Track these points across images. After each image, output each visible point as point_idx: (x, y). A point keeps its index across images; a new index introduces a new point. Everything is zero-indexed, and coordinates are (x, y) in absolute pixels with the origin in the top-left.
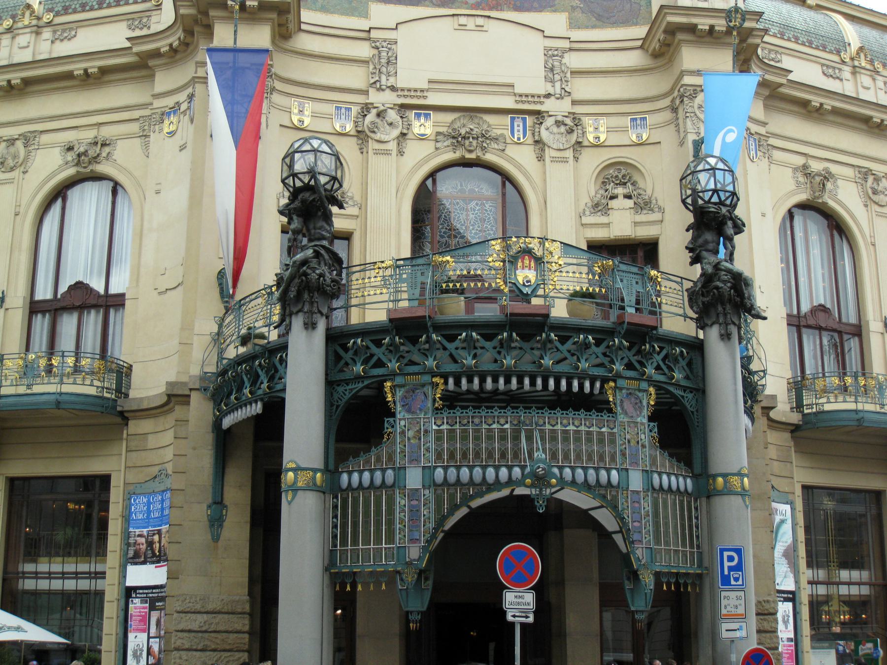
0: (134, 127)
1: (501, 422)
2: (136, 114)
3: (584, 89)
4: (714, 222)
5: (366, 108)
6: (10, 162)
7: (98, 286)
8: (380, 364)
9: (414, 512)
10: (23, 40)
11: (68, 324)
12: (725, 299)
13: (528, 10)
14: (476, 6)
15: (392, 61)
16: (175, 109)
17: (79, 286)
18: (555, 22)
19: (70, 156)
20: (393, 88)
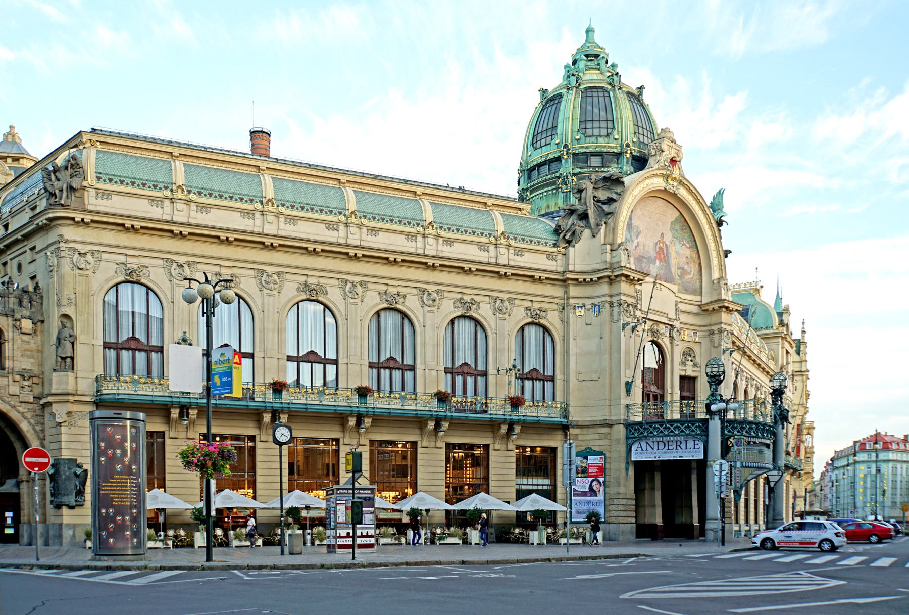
0: (555, 306)
2: (557, 301)
13: (670, 283)
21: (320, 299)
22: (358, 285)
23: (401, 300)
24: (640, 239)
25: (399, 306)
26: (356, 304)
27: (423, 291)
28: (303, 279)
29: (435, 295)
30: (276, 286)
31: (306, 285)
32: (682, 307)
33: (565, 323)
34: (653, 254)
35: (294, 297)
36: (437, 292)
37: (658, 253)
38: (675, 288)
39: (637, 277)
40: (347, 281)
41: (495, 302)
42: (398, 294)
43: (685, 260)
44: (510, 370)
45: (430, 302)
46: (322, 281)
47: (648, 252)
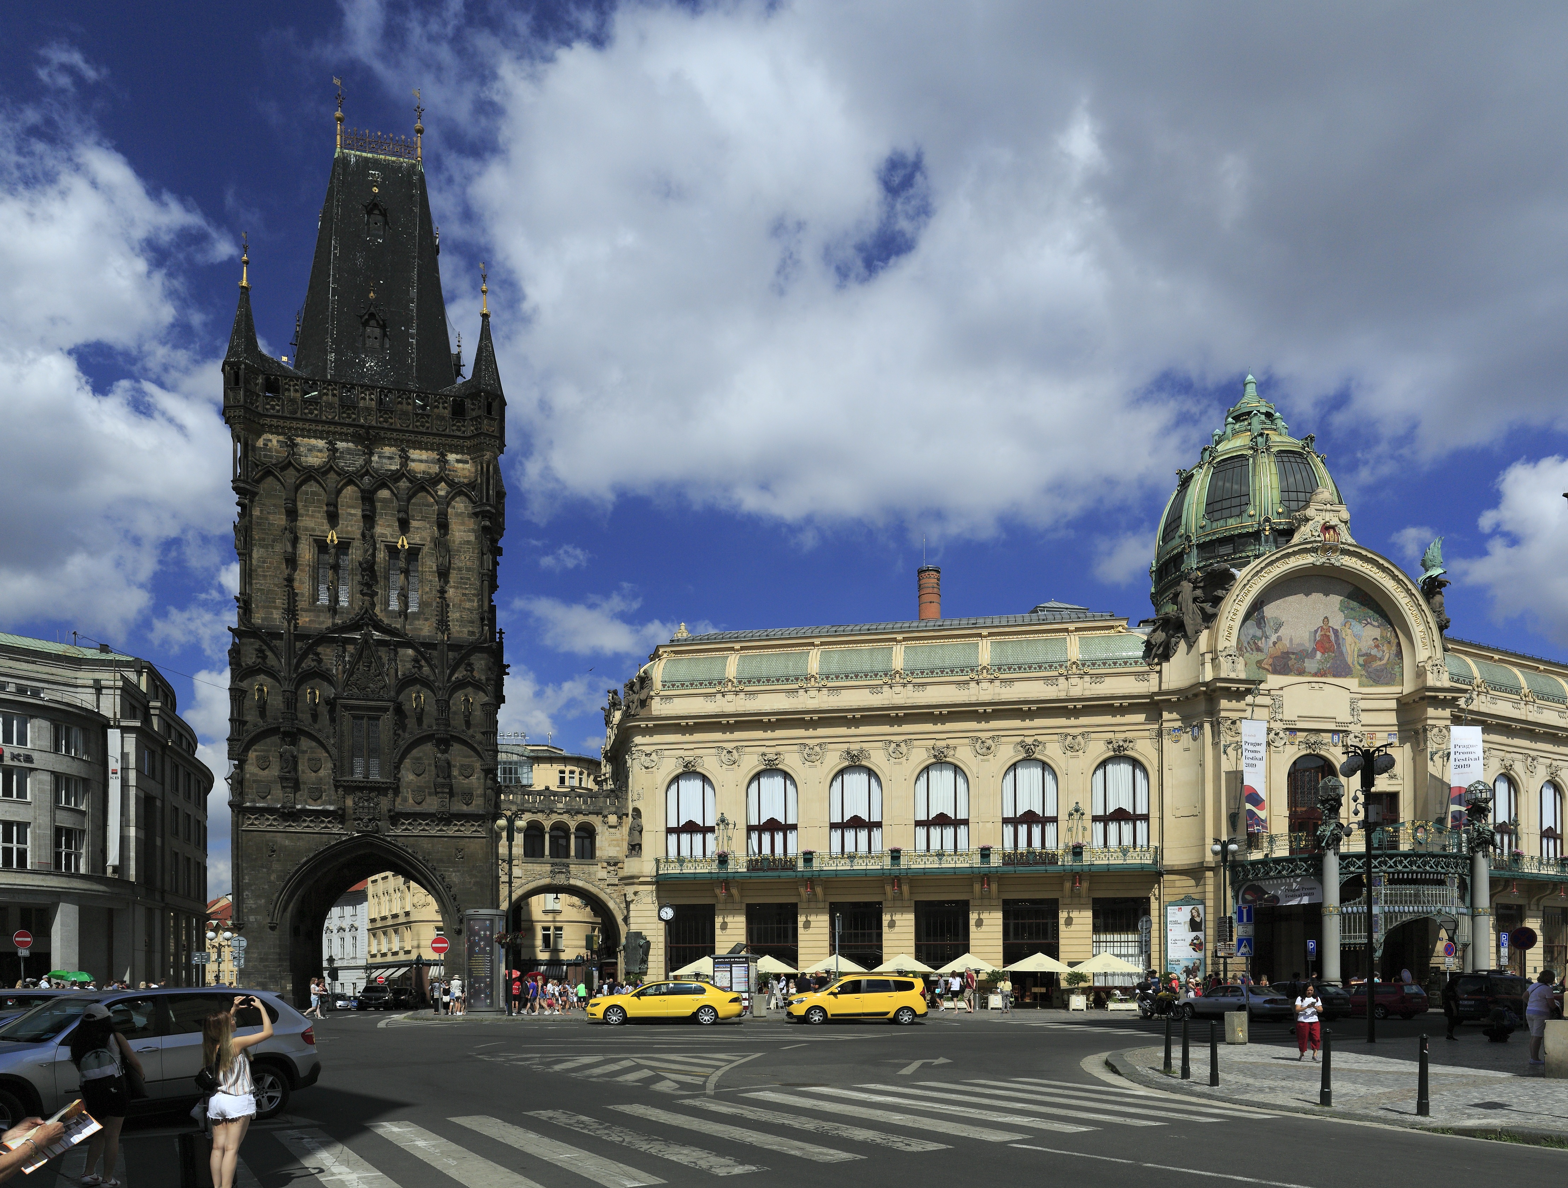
0: (1147, 733)
5: (1269, 730)
14: (1315, 675)
15: (1281, 706)
19: (1110, 746)
20: (1281, 720)
21: (863, 763)
22: (903, 744)
23: (952, 752)
26: (900, 763)
27: (978, 738)
28: (845, 747)
29: (990, 741)
32: (1363, 704)
34: (1309, 646)
36: (993, 738)
38: (1352, 683)
40: (890, 742)
41: (1065, 739)
43: (1371, 643)
47: (1303, 645)
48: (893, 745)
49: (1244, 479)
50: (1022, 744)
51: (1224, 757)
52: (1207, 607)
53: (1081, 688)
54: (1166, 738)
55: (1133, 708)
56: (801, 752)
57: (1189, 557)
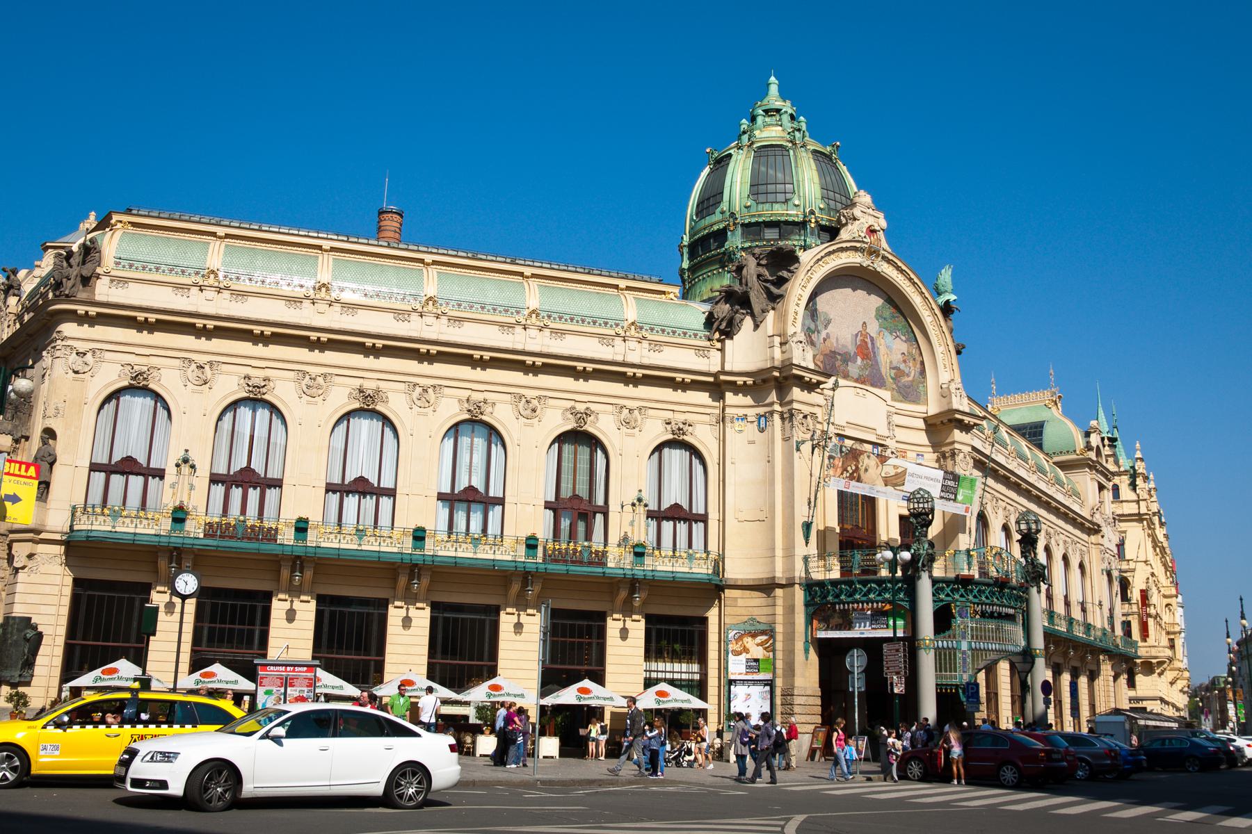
0: (707, 418)
1: (991, 625)
3: (901, 435)
4: (1028, 541)
6: (633, 424)
7: (686, 506)
8: (948, 595)
9: (964, 659)
10: (632, 344)
11: (667, 526)
12: (1037, 574)
14: (857, 381)
16: (745, 417)
17: (676, 506)
18: (886, 394)
19: (669, 427)
21: (378, 408)
22: (430, 390)
23: (490, 409)
24: (830, 329)
25: (484, 418)
26: (426, 415)
28: (358, 382)
29: (535, 402)
30: (320, 392)
31: (361, 391)
33: (723, 441)
34: (852, 349)
35: (343, 406)
36: (539, 398)
37: (859, 347)
39: (815, 378)
42: (485, 402)
43: (900, 356)
44: (633, 505)
45: (529, 412)
46: (382, 385)
48: (419, 390)
49: (786, 168)
50: (574, 413)
51: (796, 455)
52: (773, 289)
53: (638, 353)
54: (728, 425)
55: (696, 386)
56: (298, 381)
57: (733, 234)
